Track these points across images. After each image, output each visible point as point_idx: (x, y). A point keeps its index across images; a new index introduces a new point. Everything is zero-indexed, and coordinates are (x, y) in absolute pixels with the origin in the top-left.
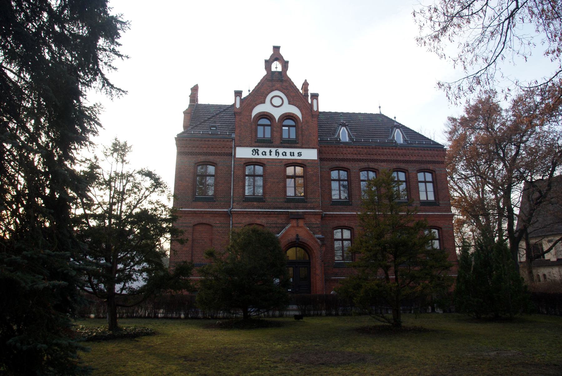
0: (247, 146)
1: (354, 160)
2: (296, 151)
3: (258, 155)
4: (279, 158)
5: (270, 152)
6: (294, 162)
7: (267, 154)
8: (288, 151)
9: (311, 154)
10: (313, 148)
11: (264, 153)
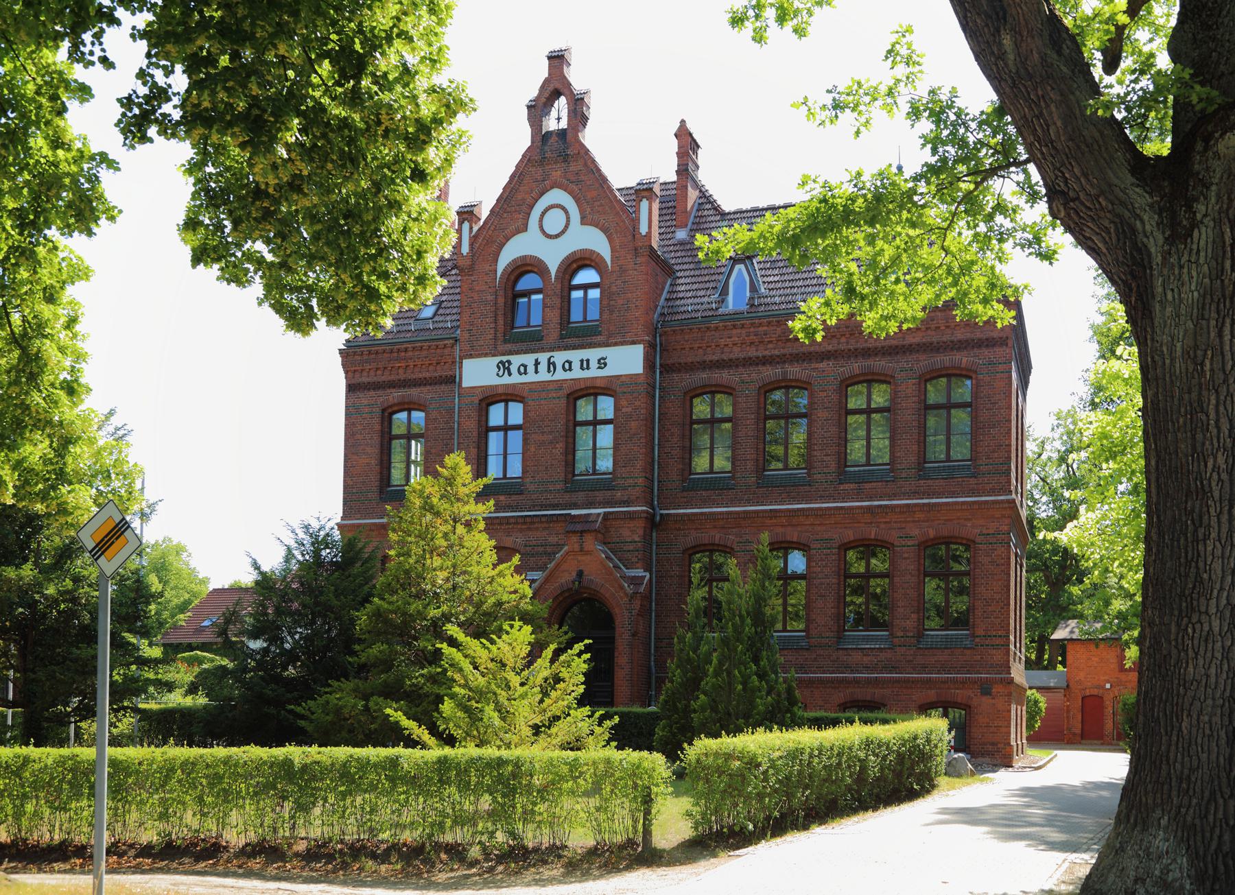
0: (486, 355)
1: (749, 362)
2: (593, 354)
3: (510, 374)
4: (556, 377)
5: (537, 363)
6: (588, 384)
7: (533, 369)
8: (576, 356)
9: (627, 360)
10: (633, 343)
11: (523, 370)
